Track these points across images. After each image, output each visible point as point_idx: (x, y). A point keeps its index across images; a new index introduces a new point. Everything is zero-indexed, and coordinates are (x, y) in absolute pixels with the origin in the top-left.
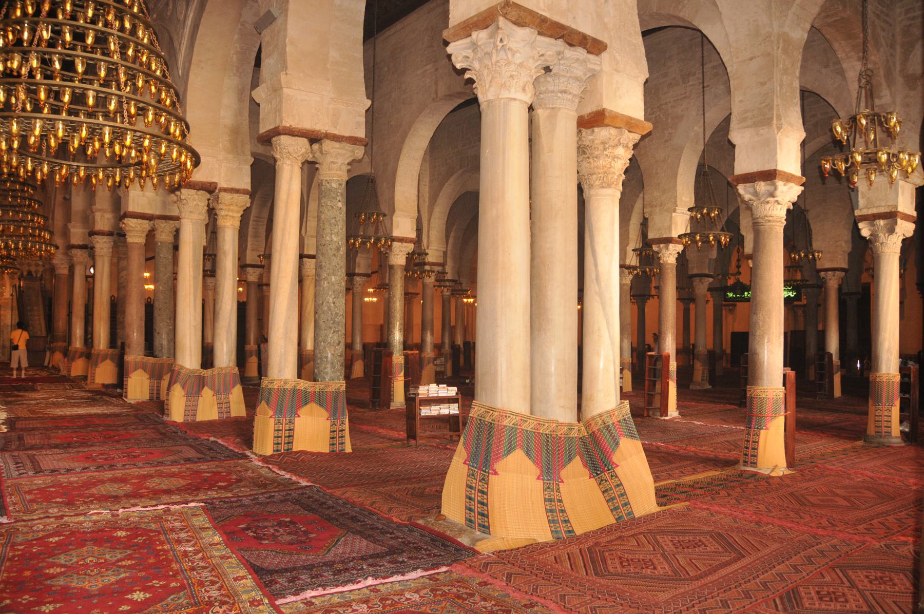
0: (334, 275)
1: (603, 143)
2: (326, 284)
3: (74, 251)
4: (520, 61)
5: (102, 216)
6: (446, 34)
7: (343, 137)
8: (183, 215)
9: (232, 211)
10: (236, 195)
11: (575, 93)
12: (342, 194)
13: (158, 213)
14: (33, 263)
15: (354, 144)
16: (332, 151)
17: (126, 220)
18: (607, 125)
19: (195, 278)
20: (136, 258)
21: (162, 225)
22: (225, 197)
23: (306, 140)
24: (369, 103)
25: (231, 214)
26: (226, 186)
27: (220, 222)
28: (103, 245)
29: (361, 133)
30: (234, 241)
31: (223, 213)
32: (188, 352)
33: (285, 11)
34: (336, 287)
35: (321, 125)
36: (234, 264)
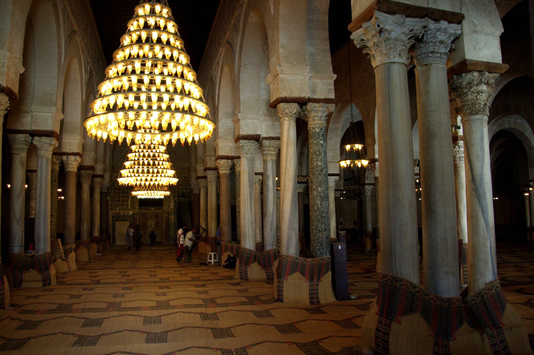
0: (320, 187)
1: (469, 83)
2: (315, 193)
3: (199, 180)
4: (395, 37)
5: (210, 159)
6: (350, 27)
7: (320, 99)
8: (242, 156)
9: (271, 150)
10: (272, 141)
11: (443, 51)
12: (322, 135)
17: (218, 161)
18: (471, 71)
22: (266, 143)
23: (296, 104)
24: (335, 76)
25: (270, 152)
29: (332, 96)
31: (266, 152)
32: (248, 237)
34: (322, 194)
35: (306, 94)
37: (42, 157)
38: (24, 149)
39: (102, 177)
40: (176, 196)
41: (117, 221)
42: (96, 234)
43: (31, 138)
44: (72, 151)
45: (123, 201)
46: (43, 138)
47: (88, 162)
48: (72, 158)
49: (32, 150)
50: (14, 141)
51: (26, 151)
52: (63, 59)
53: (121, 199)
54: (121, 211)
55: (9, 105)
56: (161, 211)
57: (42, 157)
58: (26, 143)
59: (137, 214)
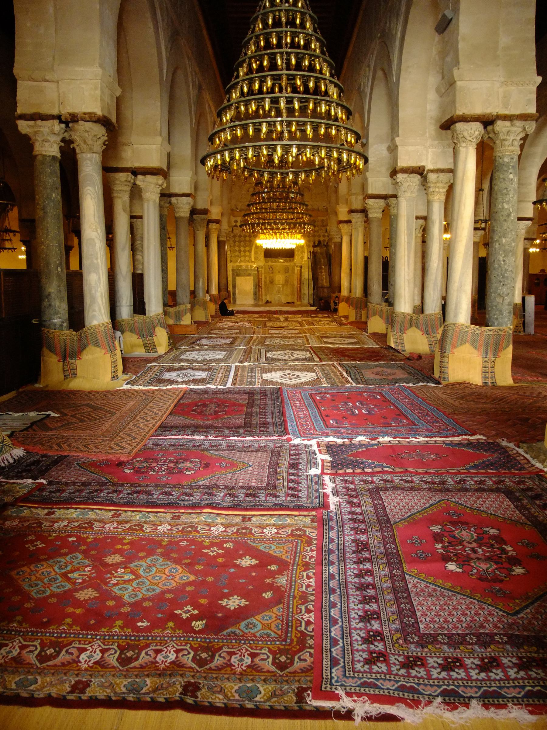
3: (341, 226)
5: (356, 198)
7: (513, 116)
9: (438, 187)
13: (390, 193)
14: (322, 235)
15: (526, 120)
16: (503, 130)
21: (392, 201)
22: (432, 177)
24: (539, 79)
25: (437, 190)
26: (432, 168)
29: (532, 110)
30: (440, 211)
31: (431, 190)
33: (456, 10)
37: (148, 200)
38: (126, 191)
39: (218, 222)
41: (238, 276)
43: (133, 177)
44: (181, 192)
45: (245, 251)
46: (149, 177)
48: (184, 200)
49: (136, 193)
50: (114, 181)
53: (242, 249)
54: (242, 264)
55: (106, 138)
56: (292, 263)
57: (148, 200)
58: (128, 183)
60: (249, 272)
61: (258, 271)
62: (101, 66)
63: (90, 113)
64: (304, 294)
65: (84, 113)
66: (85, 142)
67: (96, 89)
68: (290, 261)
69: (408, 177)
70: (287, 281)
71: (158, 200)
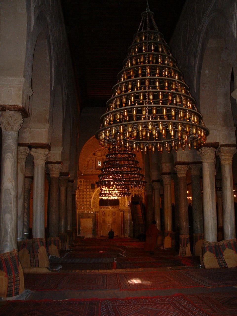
3: (154, 183)
8: (203, 161)
10: (229, 148)
17: (176, 166)
19: (212, 192)
20: (182, 185)
27: (222, 162)
28: (166, 179)
31: (223, 158)
32: (210, 231)
36: (231, 184)
37: (38, 165)
39: (72, 181)
40: (130, 197)
41: (81, 218)
42: (69, 228)
43: (29, 150)
45: (86, 201)
46: (39, 149)
47: (65, 170)
51: (25, 160)
52: (53, 84)
56: (117, 209)
57: (38, 165)
58: (25, 154)
59: (98, 213)
60: (90, 215)
61: (95, 215)
62: (24, 76)
63: (14, 105)
64: (126, 230)
65: (11, 105)
66: (9, 124)
67: (19, 90)
68: (116, 208)
69: (209, 150)
70: (114, 221)
71: (44, 165)
